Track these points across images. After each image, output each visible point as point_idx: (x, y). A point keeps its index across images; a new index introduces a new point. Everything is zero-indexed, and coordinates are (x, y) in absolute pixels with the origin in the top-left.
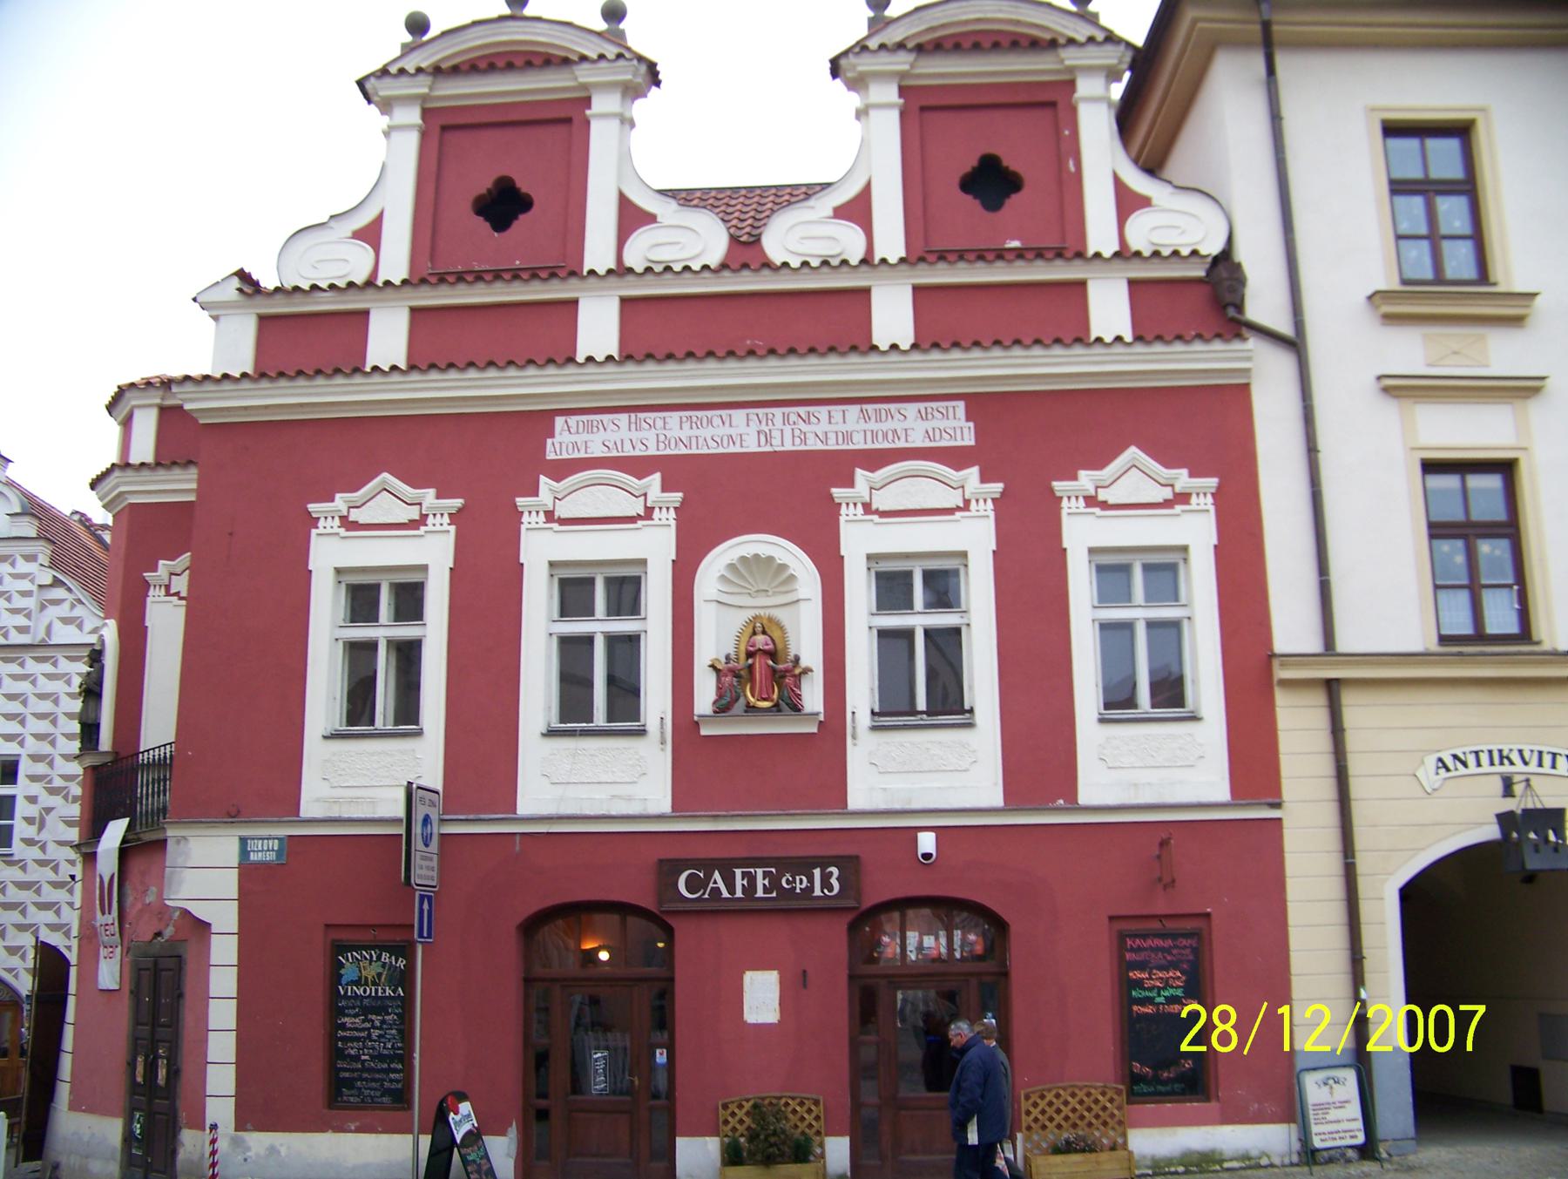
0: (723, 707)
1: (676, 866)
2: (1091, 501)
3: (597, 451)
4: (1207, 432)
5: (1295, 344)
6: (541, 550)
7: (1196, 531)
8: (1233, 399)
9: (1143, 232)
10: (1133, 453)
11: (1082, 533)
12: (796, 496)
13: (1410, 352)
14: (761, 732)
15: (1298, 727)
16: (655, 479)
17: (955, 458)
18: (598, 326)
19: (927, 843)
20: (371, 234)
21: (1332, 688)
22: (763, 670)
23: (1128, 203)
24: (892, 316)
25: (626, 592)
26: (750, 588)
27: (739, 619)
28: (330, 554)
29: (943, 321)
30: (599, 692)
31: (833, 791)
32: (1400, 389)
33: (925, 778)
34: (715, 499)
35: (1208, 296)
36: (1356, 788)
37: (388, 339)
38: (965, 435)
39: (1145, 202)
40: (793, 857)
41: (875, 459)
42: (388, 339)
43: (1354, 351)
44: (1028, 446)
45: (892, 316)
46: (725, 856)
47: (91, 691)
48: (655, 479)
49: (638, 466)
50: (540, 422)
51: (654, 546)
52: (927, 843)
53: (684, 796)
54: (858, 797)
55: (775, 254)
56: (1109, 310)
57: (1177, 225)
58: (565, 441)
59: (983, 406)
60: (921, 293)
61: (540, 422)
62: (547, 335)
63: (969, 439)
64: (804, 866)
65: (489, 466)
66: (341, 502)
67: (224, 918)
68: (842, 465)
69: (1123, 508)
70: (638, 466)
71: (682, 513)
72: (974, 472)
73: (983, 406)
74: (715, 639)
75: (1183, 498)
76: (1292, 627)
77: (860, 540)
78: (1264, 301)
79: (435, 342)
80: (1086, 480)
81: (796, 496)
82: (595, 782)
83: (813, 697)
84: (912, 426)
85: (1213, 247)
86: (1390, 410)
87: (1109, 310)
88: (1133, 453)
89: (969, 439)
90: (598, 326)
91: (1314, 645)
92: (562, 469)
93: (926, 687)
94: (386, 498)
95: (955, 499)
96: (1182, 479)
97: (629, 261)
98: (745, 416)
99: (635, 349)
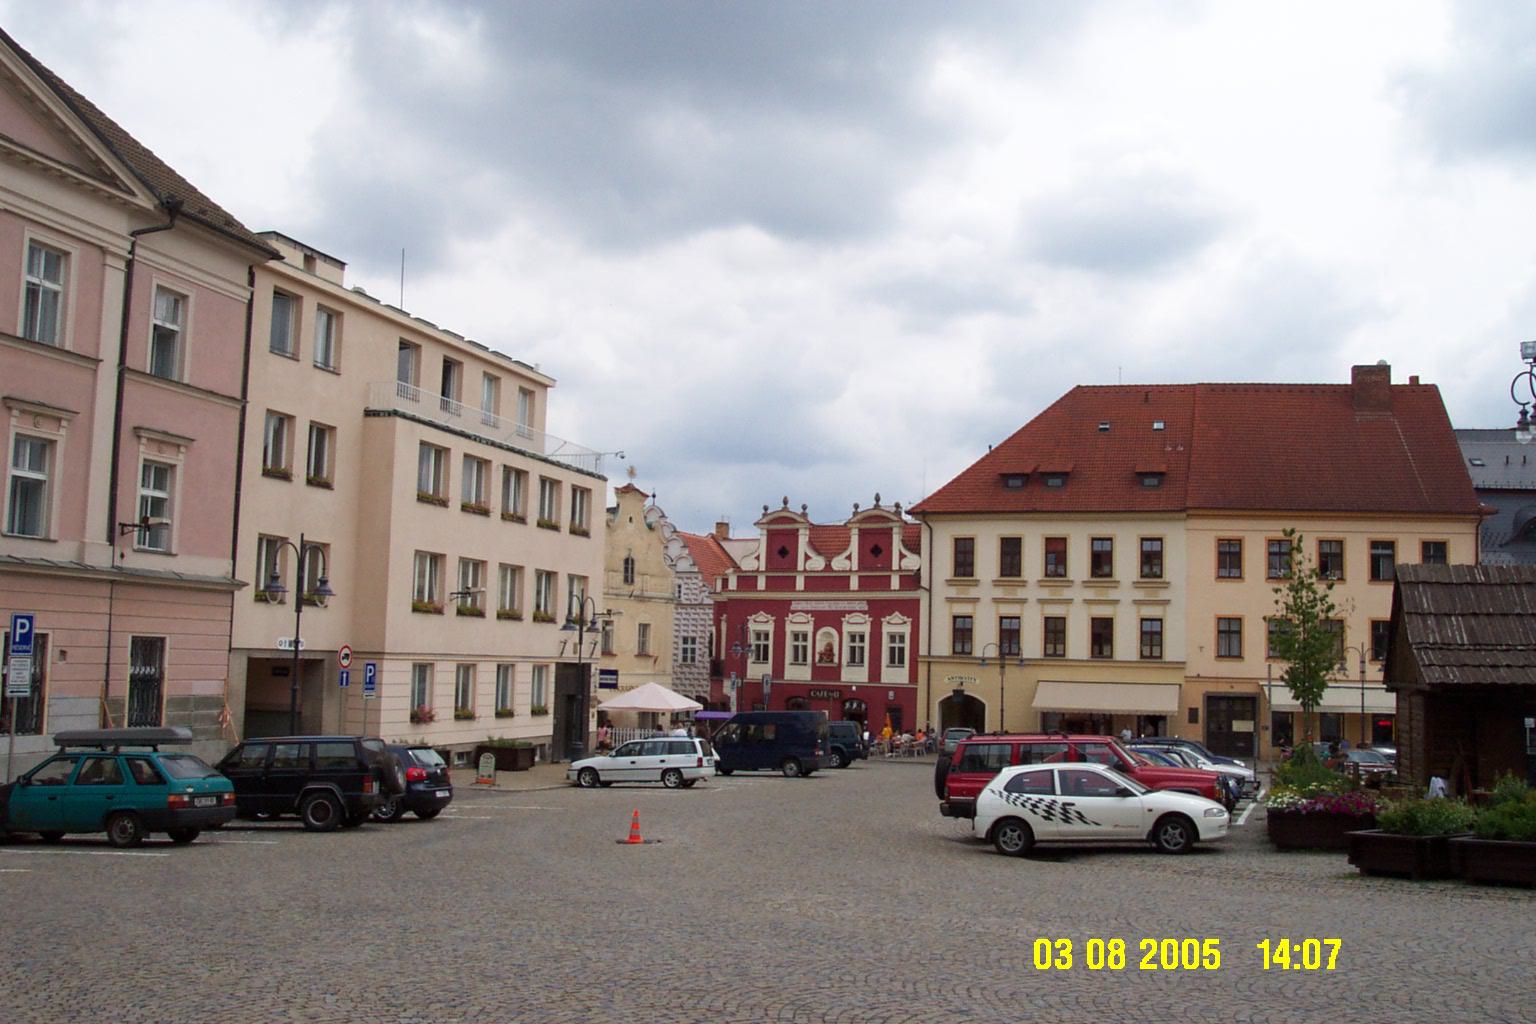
0: (820, 661)
1: (811, 690)
2: (888, 623)
3: (800, 609)
4: (910, 609)
5: (930, 590)
6: (789, 628)
7: (907, 630)
9: (905, 563)
10: (897, 613)
11: (886, 629)
12: (833, 619)
13: (953, 592)
14: (827, 667)
15: (922, 670)
16: (810, 615)
17: (864, 612)
18: (800, 583)
19: (854, 688)
20: (758, 558)
21: (929, 663)
22: (828, 653)
23: (902, 556)
24: (854, 583)
25: (805, 638)
26: (826, 636)
27: (825, 643)
28: (752, 627)
29: (865, 583)
30: (799, 656)
31: (838, 678)
32: (950, 600)
33: (855, 676)
34: (822, 619)
35: (912, 580)
36: (932, 682)
37: (761, 583)
38: (865, 607)
39: (905, 556)
40: (831, 689)
42: (761, 583)
43: (941, 591)
44: (878, 611)
45: (854, 583)
46: (818, 689)
47: (711, 642)
48: (810, 615)
49: (807, 612)
50: (789, 602)
51: (809, 628)
52: (854, 688)
53: (814, 677)
54: (843, 679)
55: (835, 568)
56: (895, 583)
57: (911, 562)
58: (794, 606)
59: (870, 602)
60: (860, 577)
61: (789, 602)
62: (790, 584)
63: (866, 609)
64: (832, 692)
65: (780, 610)
66: (754, 616)
68: (843, 613)
69: (895, 624)
70: (807, 612)
71: (815, 622)
72: (867, 616)
73: (870, 602)
74: (820, 647)
75: (905, 623)
76: (923, 650)
77: (846, 628)
78: (924, 583)
79: (772, 584)
80: (888, 618)
81: (833, 619)
82: (798, 674)
83: (836, 660)
84: (857, 606)
85: (917, 568)
86: (948, 605)
87: (895, 583)
88: (897, 613)
89: (866, 609)
90: (800, 583)
91: (926, 654)
92: (793, 612)
93: (855, 658)
94: (762, 616)
95: (863, 621)
96: (905, 618)
97: (807, 568)
98: (827, 602)
99: (808, 587)
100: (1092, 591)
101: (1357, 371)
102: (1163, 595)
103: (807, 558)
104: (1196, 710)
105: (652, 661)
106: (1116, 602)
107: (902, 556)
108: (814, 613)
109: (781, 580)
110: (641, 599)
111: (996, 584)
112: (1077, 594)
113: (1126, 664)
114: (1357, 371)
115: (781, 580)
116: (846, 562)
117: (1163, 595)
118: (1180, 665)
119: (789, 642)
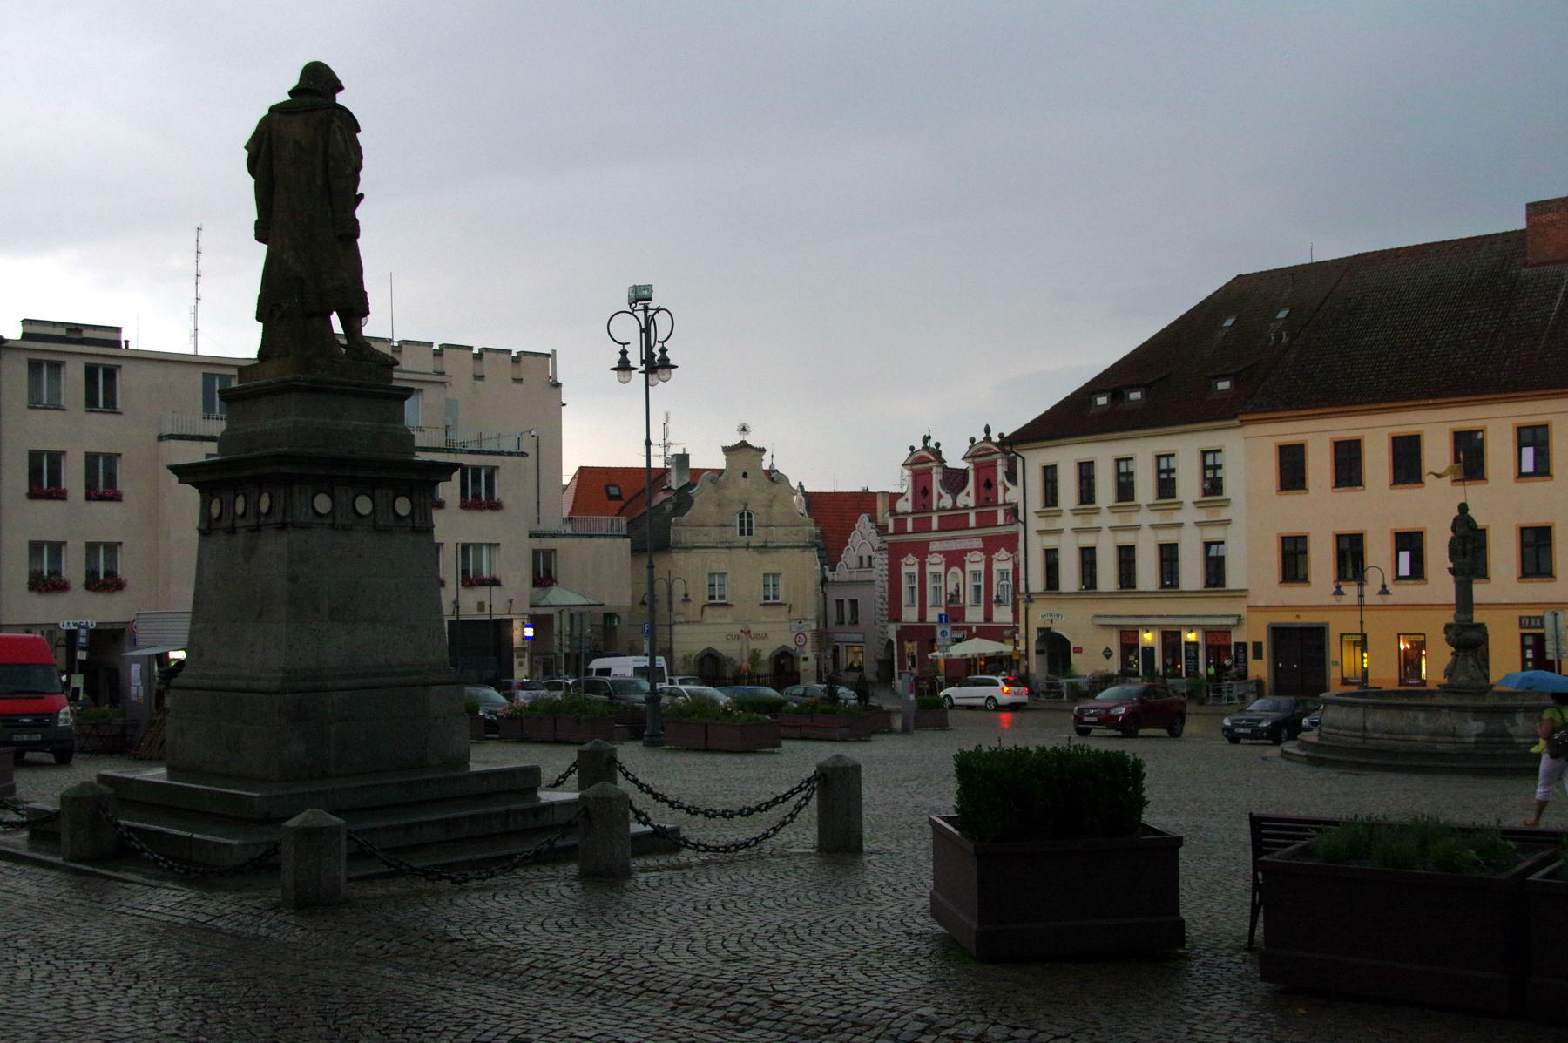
5: (1025, 523)
6: (929, 569)
8: (1015, 536)
23: (1006, 489)
24: (972, 521)
26: (954, 578)
28: (905, 570)
31: (963, 619)
41: (971, 551)
44: (990, 546)
45: (972, 521)
49: (940, 552)
50: (926, 544)
51: (941, 569)
58: (934, 547)
59: (985, 539)
61: (926, 544)
65: (921, 551)
67: (894, 640)
68: (964, 552)
70: (940, 552)
73: (985, 539)
74: (951, 588)
77: (969, 567)
87: (1001, 519)
100: (1204, 511)
101: (1534, 209)
102: (1224, 514)
103: (940, 497)
104: (1152, 649)
105: (785, 609)
106: (1180, 525)
107: (1006, 489)
108: (946, 554)
109: (922, 526)
110: (764, 548)
111: (1075, 512)
112: (1145, 518)
113: (1192, 594)
114: (1534, 209)
115: (922, 526)
116: (967, 498)
117: (1224, 514)
118: (1241, 594)
119: (930, 584)
